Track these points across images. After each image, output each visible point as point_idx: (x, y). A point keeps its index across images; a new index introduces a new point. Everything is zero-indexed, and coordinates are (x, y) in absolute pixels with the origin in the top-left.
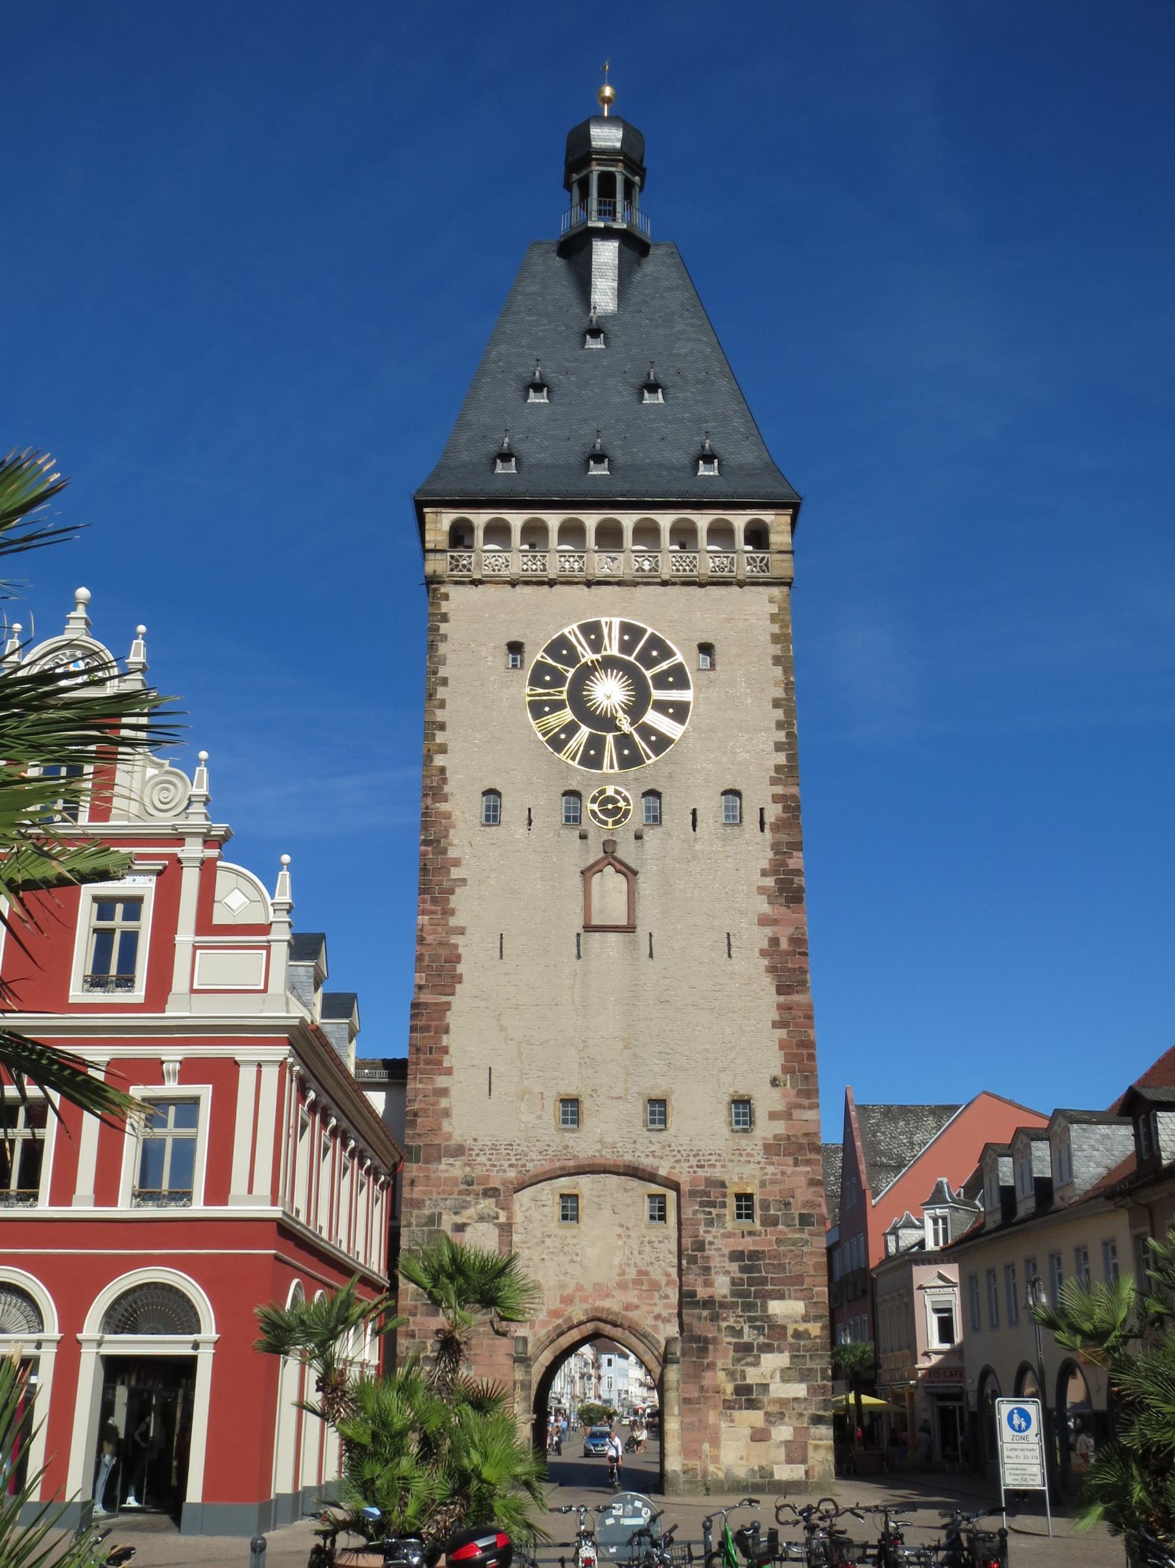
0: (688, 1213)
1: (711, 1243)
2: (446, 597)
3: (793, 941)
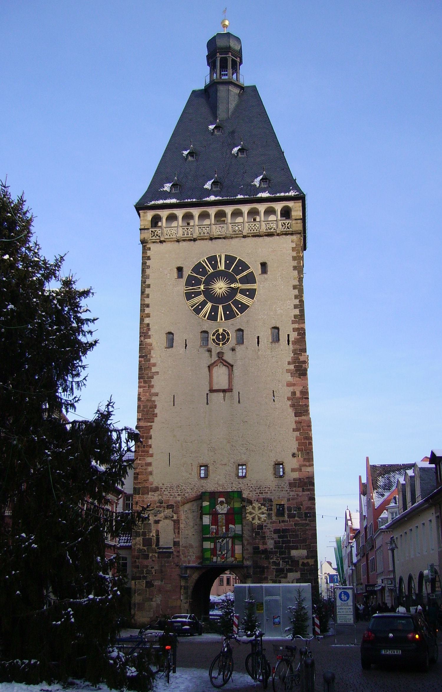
1: (265, 526)
2: (149, 249)
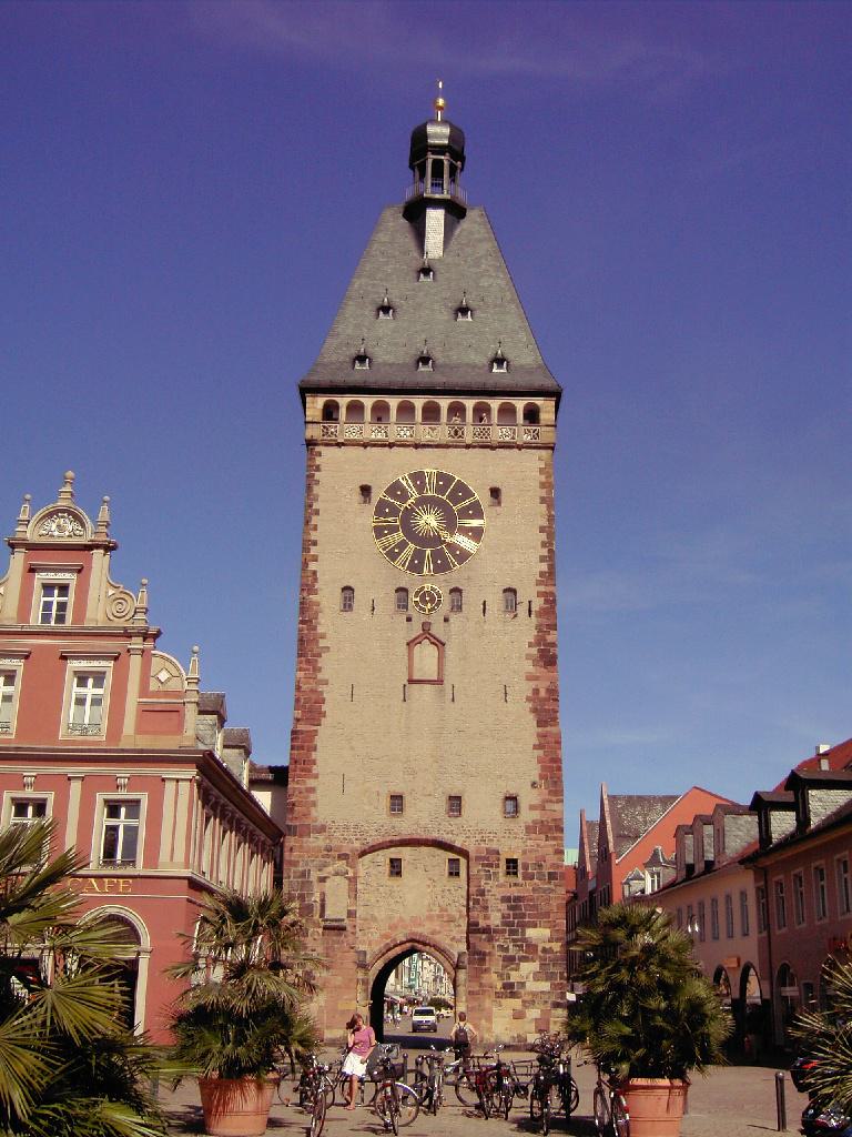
0: (474, 871)
1: (489, 891)
2: (320, 454)
3: (548, 690)
